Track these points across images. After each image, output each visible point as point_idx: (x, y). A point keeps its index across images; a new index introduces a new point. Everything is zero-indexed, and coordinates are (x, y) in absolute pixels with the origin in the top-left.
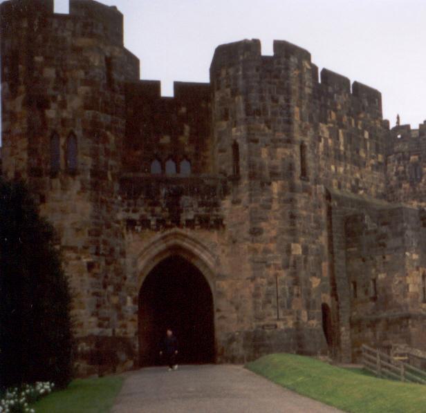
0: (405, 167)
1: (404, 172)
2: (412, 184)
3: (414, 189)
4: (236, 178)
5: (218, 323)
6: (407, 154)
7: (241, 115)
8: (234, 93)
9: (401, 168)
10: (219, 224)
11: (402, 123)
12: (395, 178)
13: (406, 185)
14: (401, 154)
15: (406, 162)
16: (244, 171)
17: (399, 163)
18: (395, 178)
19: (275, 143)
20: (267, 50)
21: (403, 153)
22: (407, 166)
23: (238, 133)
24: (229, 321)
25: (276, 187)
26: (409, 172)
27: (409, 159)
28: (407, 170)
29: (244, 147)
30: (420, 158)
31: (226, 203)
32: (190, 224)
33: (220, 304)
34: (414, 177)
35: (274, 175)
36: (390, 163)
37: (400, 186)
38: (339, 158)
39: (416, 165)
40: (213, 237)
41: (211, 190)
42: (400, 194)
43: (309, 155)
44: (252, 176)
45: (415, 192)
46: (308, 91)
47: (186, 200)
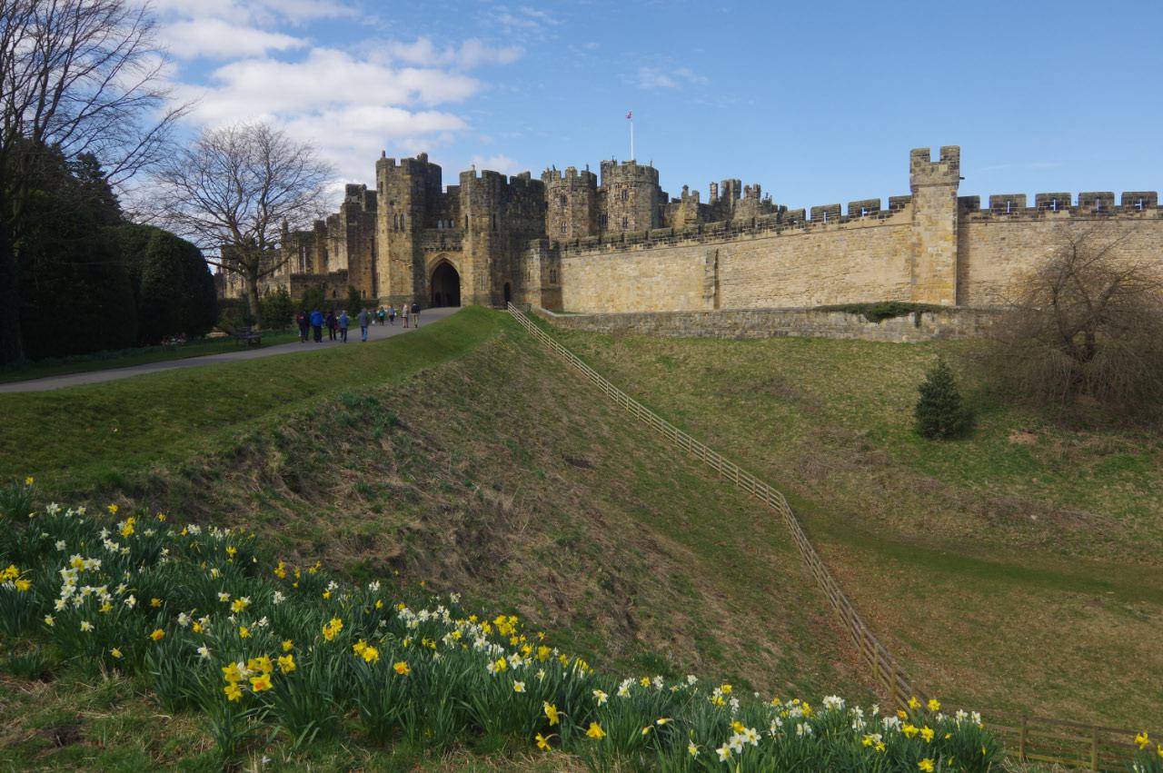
4: (467, 232)
5: (462, 291)
7: (469, 204)
8: (466, 194)
10: (461, 249)
13: (620, 203)
16: (470, 228)
19: (482, 216)
20: (479, 175)
23: (468, 212)
24: (466, 291)
25: (482, 234)
29: (469, 218)
31: (464, 241)
32: (449, 250)
33: (461, 283)
35: (482, 229)
38: (517, 216)
40: (459, 255)
41: (457, 236)
43: (498, 220)
44: (473, 230)
46: (497, 191)
47: (447, 240)
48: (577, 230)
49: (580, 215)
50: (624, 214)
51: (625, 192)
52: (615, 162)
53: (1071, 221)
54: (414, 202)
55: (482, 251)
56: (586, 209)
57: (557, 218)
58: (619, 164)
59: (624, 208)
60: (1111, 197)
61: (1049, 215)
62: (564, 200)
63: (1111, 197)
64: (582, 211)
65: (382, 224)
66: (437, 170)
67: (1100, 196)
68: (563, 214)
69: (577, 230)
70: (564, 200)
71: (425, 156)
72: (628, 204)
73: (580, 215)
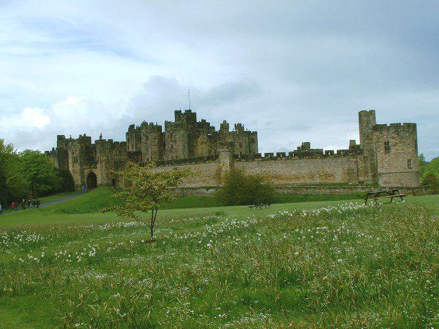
24: (99, 182)
51: (172, 134)
52: (180, 111)
53: (262, 161)
54: (81, 153)
55: (104, 168)
56: (156, 141)
58: (183, 112)
60: (273, 154)
61: (256, 159)
62: (147, 137)
63: (273, 154)
65: (70, 160)
66: (90, 138)
67: (270, 154)
70: (147, 137)
71: (85, 135)
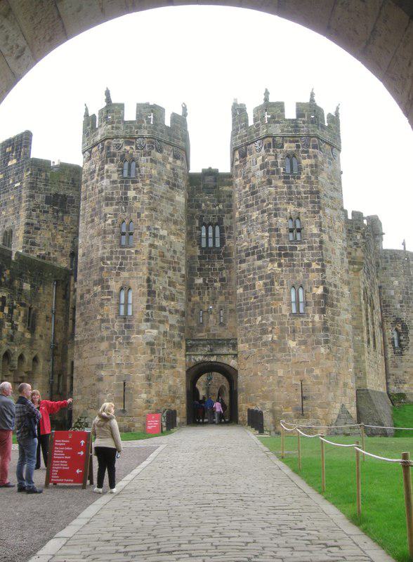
0: (276, 156)
1: (275, 164)
2: (286, 179)
3: (290, 187)
6: (279, 140)
9: (271, 159)
11: (272, 99)
12: (260, 173)
14: (271, 140)
15: (278, 150)
17: (268, 151)
18: (260, 173)
21: (274, 137)
22: (280, 156)
26: (283, 165)
27: (282, 147)
28: (279, 161)
30: (298, 147)
34: (288, 171)
36: (251, 154)
37: (269, 182)
39: (290, 156)
42: (270, 194)
45: (291, 193)
48: (159, 243)
49: (167, 209)
50: (291, 208)
57: (109, 210)
59: (290, 196)
64: (171, 200)
68: (125, 200)
69: (159, 243)
72: (301, 185)
73: (167, 209)
